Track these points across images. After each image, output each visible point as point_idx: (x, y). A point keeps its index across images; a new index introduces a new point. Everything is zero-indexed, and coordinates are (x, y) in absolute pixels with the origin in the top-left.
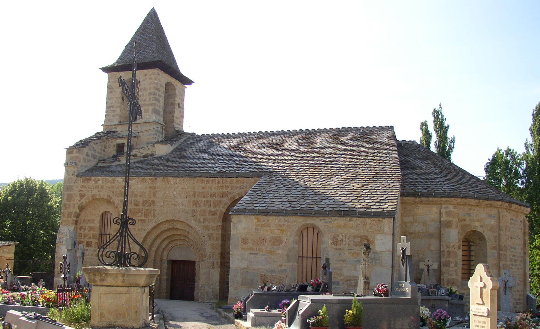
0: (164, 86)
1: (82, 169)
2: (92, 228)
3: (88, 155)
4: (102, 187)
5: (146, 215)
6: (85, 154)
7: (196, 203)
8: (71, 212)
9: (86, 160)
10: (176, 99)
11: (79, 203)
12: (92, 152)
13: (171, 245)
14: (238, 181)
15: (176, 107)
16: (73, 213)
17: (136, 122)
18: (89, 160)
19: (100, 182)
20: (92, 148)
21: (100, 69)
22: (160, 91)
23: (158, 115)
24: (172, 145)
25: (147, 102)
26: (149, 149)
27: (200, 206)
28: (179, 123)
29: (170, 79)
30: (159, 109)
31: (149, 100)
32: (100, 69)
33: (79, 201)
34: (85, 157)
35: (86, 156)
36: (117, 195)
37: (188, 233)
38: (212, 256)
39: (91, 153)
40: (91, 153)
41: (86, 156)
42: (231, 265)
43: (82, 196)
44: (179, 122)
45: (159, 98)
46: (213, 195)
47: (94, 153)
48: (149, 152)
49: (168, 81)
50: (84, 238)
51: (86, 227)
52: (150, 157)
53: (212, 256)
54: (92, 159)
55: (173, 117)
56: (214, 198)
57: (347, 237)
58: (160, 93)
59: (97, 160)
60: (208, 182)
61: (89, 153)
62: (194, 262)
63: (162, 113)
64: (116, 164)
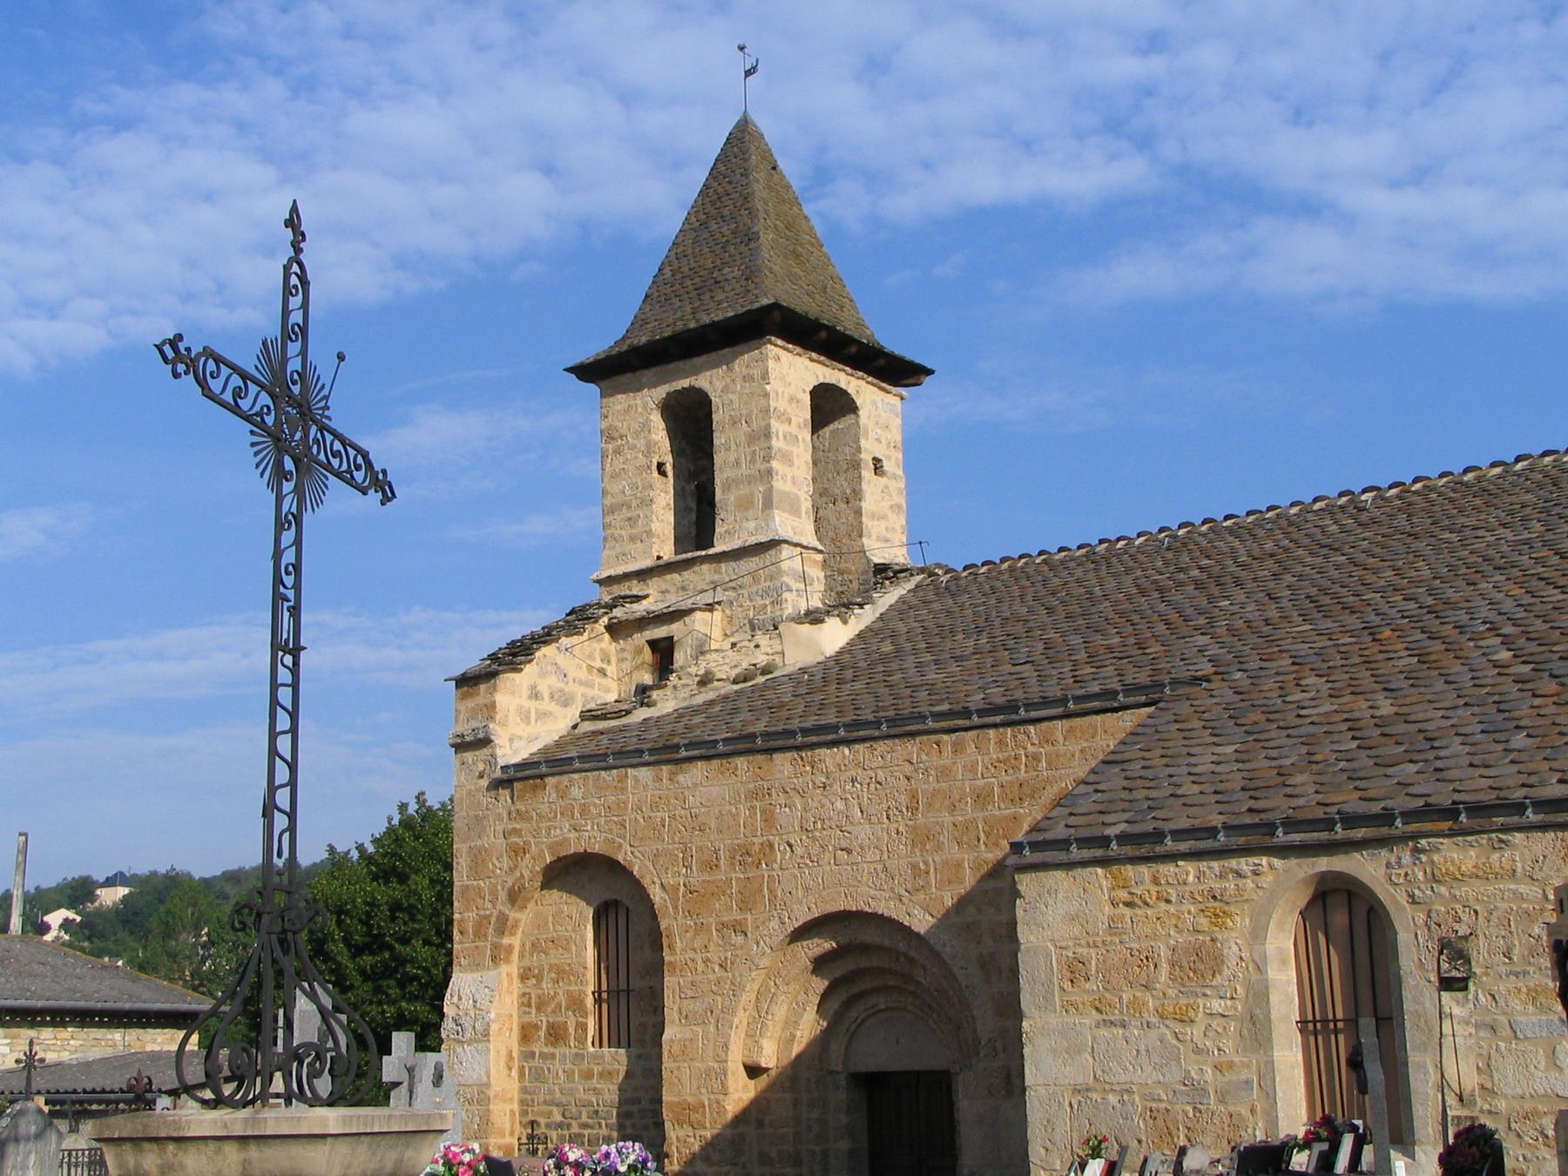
0: (807, 399)
1: (516, 751)
2: (564, 971)
3: (535, 695)
4: (584, 810)
5: (746, 904)
6: (525, 692)
7: (922, 838)
8: (487, 917)
9: (529, 712)
10: (863, 443)
11: (510, 880)
12: (554, 681)
13: (853, 1013)
14: (1071, 730)
15: (867, 473)
16: (493, 920)
17: (711, 551)
18: (543, 715)
19: (576, 792)
20: (549, 668)
21: (568, 370)
22: (790, 421)
23: (791, 513)
24: (845, 622)
25: (744, 470)
26: (757, 646)
27: (939, 847)
28: (884, 533)
29: (828, 371)
30: (795, 491)
31: (753, 461)
32: (568, 370)
33: (512, 870)
34: (527, 703)
35: (530, 697)
36: (640, 835)
37: (911, 961)
38: (999, 1045)
39: (550, 687)
40: (550, 687)
41: (530, 697)
42: (1030, 1076)
43: (518, 851)
44: (887, 529)
45: (789, 448)
46: (982, 798)
47: (561, 685)
48: (761, 659)
49: (821, 380)
50: (539, 1009)
51: (541, 971)
52: (761, 679)
53: (999, 1045)
54: (555, 708)
55: (859, 513)
56: (990, 807)
57: (1494, 920)
58: (793, 429)
59: (573, 714)
60: (958, 748)
61: (539, 688)
62: (388, 1106)
63: (806, 504)
64: (640, 720)
